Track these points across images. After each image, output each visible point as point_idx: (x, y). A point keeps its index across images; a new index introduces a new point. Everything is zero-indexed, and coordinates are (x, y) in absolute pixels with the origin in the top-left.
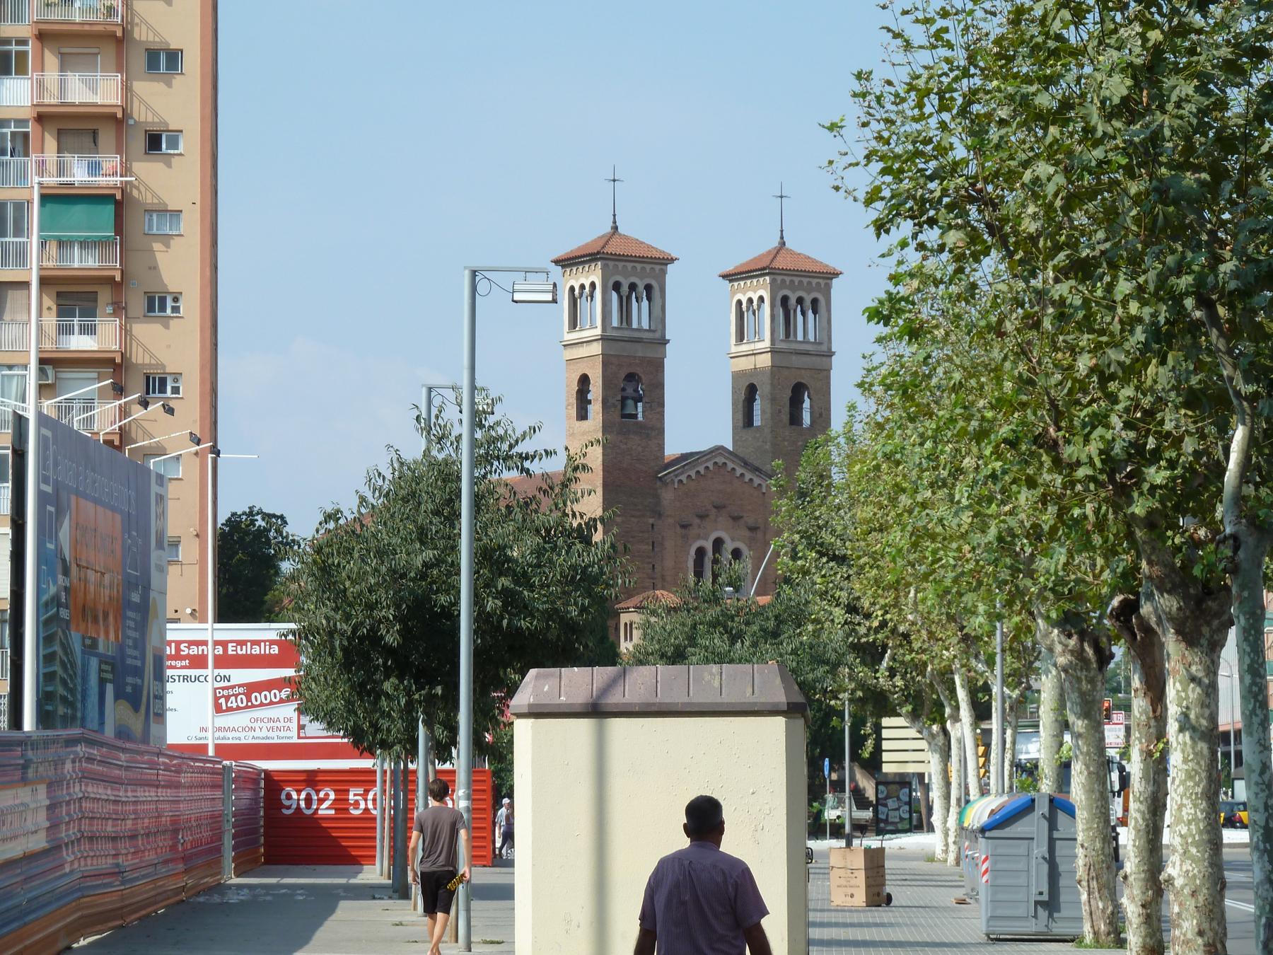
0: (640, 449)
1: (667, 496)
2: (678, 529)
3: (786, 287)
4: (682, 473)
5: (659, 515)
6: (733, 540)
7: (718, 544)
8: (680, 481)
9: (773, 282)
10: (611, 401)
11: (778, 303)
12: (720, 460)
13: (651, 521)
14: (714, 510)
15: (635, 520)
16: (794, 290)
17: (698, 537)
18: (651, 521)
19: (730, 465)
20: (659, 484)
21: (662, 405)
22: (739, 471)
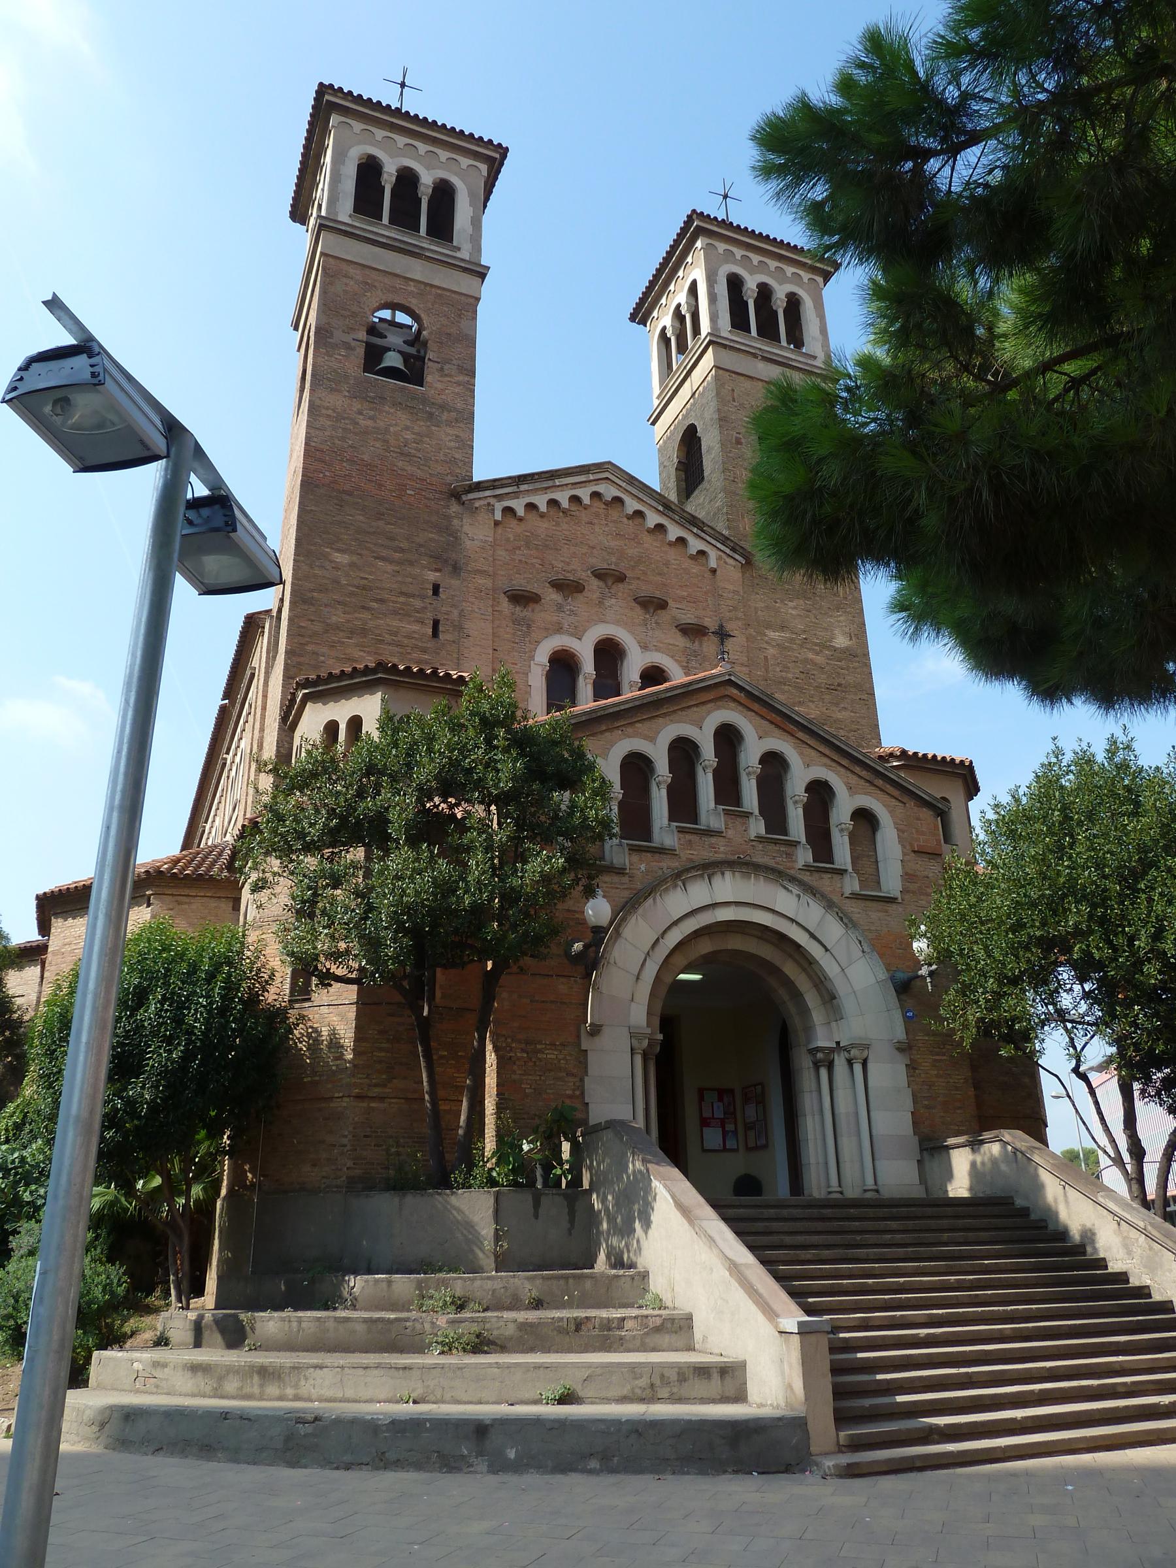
0: (409, 436)
1: (476, 533)
2: (505, 605)
3: (735, 262)
4: (516, 495)
5: (456, 569)
6: (645, 647)
7: (609, 654)
8: (508, 511)
9: (707, 248)
10: (339, 336)
11: (722, 289)
12: (609, 491)
13: (433, 576)
14: (595, 583)
15: (390, 568)
16: (753, 271)
17: (559, 629)
18: (433, 576)
19: (632, 505)
20: (455, 508)
21: (472, 373)
22: (653, 519)
